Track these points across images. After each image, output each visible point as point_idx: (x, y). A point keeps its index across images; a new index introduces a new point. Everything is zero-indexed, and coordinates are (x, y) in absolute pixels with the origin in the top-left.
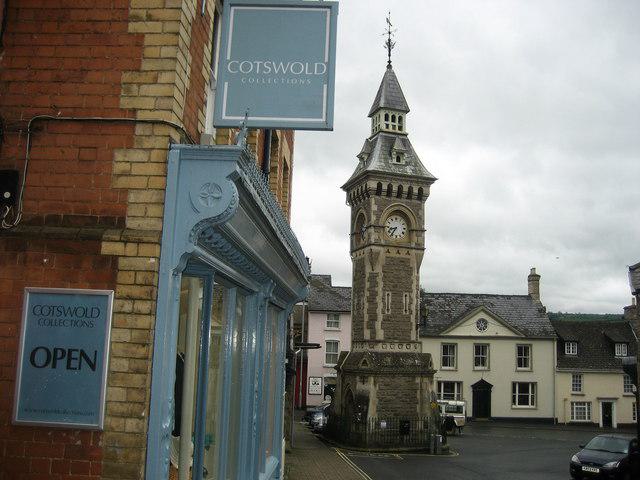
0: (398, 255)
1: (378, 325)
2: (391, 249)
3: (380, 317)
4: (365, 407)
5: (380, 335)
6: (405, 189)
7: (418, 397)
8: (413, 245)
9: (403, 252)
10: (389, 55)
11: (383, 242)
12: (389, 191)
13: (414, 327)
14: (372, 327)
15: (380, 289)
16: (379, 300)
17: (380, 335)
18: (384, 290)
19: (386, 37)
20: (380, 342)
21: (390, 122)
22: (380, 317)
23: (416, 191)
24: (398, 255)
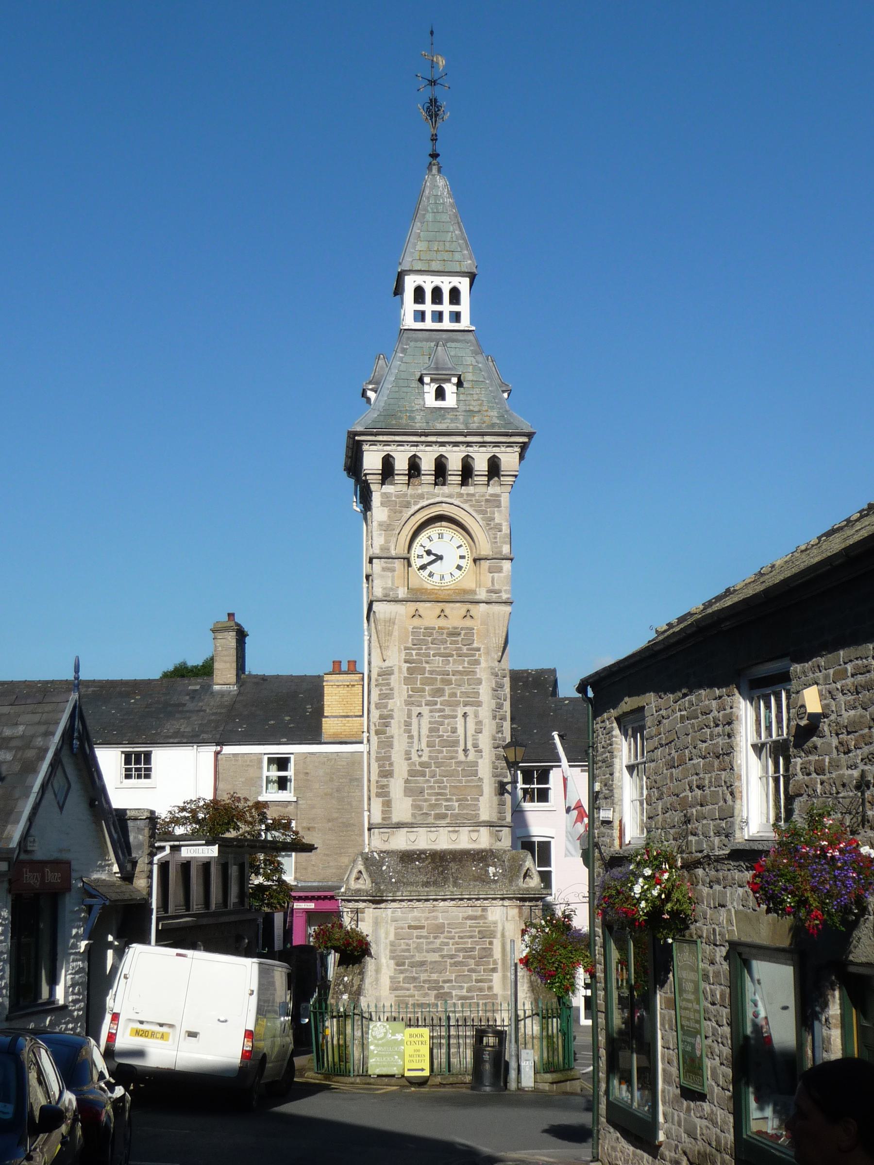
0: (442, 622)
1: (396, 787)
2: (424, 608)
3: (401, 769)
4: (356, 983)
5: (402, 809)
6: (454, 464)
7: (497, 954)
8: (482, 595)
9: (455, 612)
10: (434, 138)
11: (402, 593)
12: (414, 468)
13: (489, 787)
14: (383, 793)
15: (397, 703)
16: (396, 729)
17: (402, 809)
18: (408, 703)
19: (427, 93)
20: (399, 826)
21: (428, 307)
22: (401, 769)
23: (481, 465)
24: (442, 622)
